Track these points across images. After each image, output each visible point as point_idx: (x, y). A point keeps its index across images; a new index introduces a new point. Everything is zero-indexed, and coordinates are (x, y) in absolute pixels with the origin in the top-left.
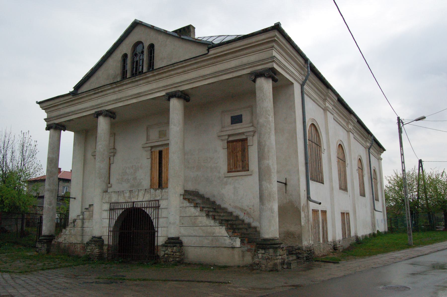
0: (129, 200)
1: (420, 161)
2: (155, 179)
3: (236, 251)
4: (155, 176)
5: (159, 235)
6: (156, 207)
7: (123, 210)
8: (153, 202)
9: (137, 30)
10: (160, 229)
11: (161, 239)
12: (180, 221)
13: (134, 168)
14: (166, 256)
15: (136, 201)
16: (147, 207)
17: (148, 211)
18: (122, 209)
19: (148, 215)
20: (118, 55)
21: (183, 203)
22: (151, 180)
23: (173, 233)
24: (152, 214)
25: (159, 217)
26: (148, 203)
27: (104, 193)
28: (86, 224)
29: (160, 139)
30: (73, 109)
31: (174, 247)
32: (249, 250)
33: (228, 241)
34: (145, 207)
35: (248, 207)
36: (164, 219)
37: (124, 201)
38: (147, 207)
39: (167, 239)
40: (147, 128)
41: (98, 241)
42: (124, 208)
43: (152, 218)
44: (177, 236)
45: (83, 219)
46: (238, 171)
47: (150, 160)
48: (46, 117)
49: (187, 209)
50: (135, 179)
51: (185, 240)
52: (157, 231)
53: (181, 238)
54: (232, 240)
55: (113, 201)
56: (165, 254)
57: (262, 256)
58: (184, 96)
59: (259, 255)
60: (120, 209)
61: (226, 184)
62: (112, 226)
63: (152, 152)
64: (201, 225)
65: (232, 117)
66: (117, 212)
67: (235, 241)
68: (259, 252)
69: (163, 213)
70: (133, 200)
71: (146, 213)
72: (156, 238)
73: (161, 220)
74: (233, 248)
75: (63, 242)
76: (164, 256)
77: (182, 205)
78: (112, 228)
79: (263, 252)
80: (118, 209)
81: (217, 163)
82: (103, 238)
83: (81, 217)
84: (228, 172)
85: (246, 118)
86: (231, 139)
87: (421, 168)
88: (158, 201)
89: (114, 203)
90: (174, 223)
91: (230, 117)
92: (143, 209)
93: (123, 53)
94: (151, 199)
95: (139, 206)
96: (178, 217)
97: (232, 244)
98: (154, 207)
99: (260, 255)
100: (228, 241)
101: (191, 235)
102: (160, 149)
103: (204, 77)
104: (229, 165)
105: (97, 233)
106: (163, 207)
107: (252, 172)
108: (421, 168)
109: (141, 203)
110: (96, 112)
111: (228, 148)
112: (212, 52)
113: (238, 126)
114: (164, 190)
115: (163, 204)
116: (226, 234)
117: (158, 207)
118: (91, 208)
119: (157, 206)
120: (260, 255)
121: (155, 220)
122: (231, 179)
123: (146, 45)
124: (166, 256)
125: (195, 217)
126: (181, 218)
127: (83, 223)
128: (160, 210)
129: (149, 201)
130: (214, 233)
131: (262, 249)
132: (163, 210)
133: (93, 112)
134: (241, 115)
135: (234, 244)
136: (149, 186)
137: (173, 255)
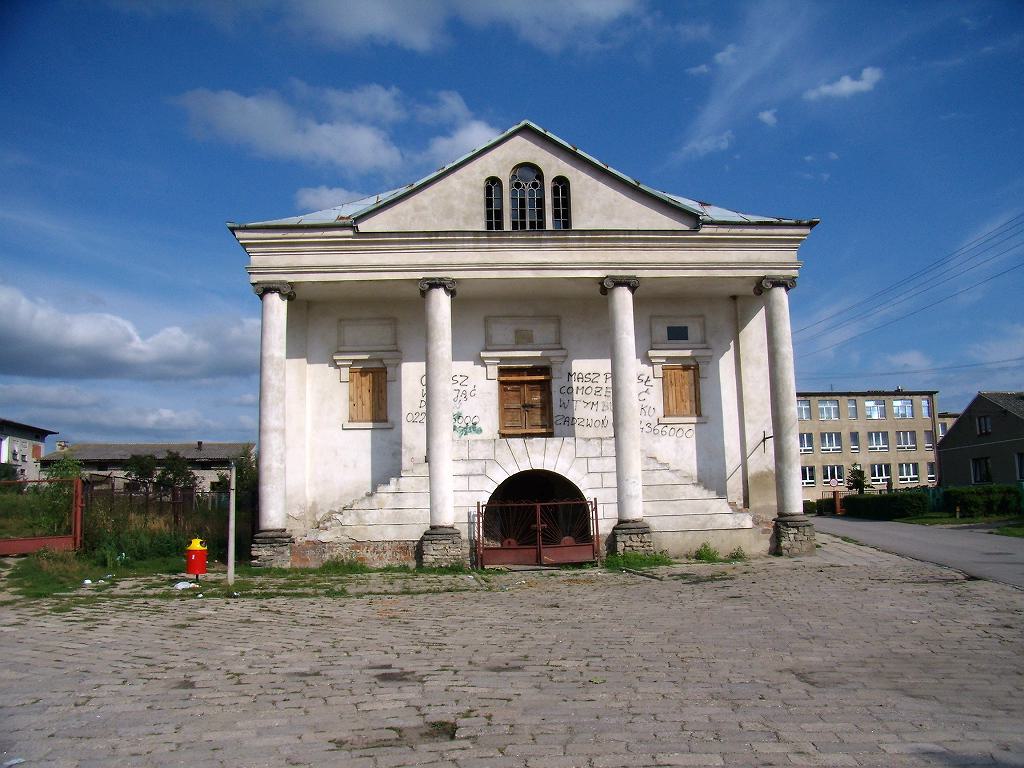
11: (604, 523)
12: (643, 492)
14: (628, 549)
21: (647, 464)
29: (520, 347)
46: (684, 416)
49: (657, 474)
51: (655, 524)
58: (631, 284)
65: (669, 328)
77: (646, 467)
85: (694, 332)
99: (792, 536)
103: (684, 266)
104: (666, 404)
107: (708, 417)
110: (428, 279)
112: (705, 230)
133: (419, 276)
134: (686, 328)
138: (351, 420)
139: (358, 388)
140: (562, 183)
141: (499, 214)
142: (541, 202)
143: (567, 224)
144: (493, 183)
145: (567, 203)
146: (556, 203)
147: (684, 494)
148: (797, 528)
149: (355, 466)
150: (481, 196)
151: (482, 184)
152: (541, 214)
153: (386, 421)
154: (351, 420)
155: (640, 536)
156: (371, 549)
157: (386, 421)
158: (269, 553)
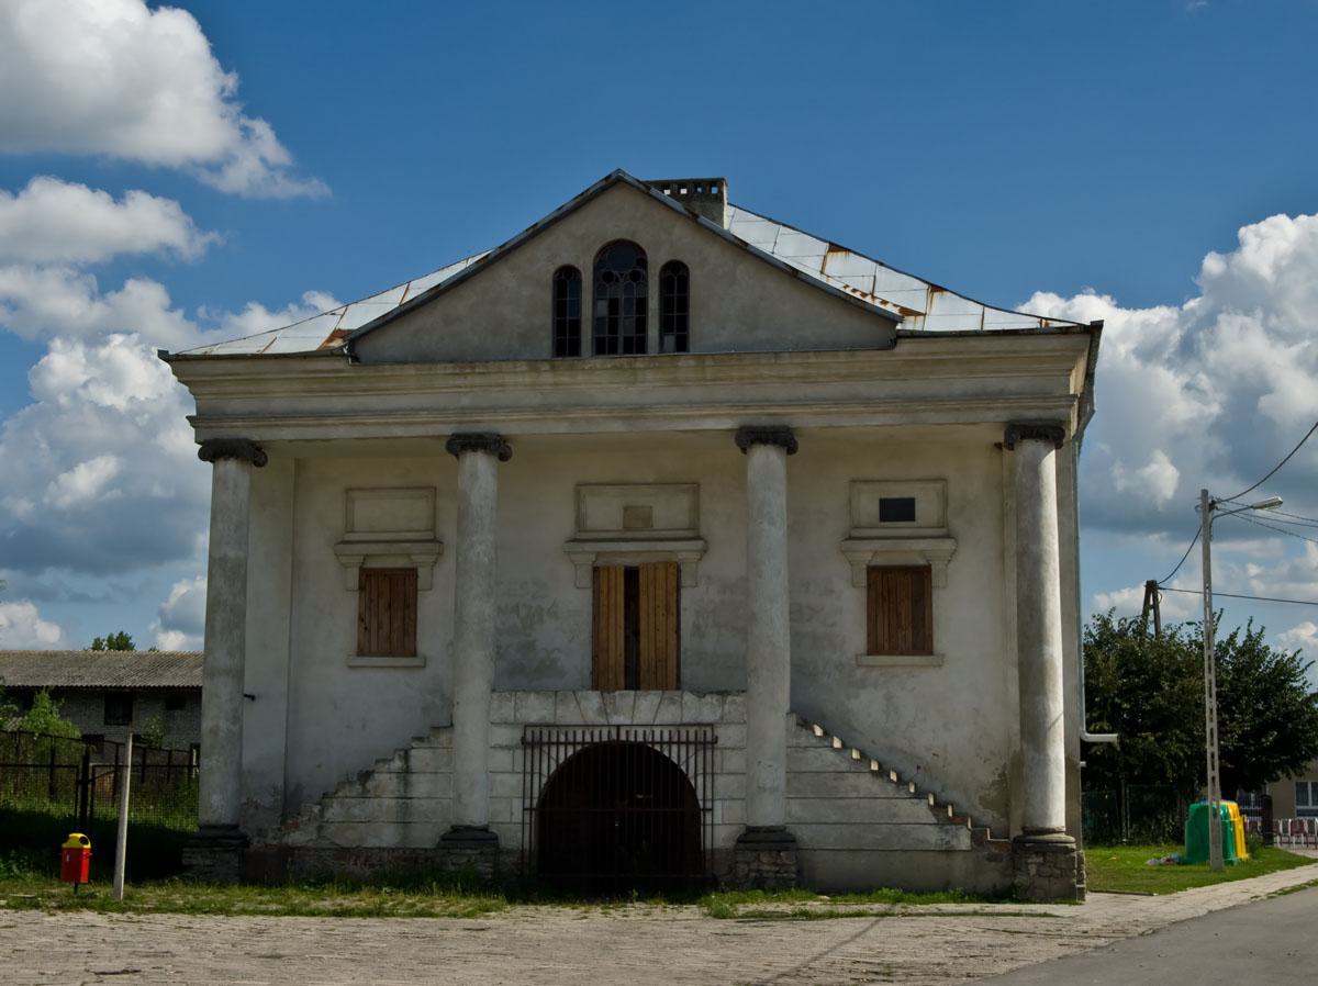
0: (602, 720)
1: (1263, 628)
2: (612, 654)
3: (959, 860)
4: (612, 644)
5: (718, 820)
6: (705, 743)
7: (579, 748)
8: (692, 731)
9: (616, 198)
10: (718, 805)
11: (721, 827)
12: (788, 782)
13: (523, 612)
15: (628, 722)
16: (670, 743)
17: (673, 754)
18: (574, 744)
19: (676, 767)
20: (542, 262)
22: (595, 657)
23: (770, 813)
24: (692, 761)
25: (717, 770)
26: (674, 730)
27: (495, 695)
28: (421, 786)
30: (338, 403)
31: (779, 851)
32: (993, 858)
33: (933, 836)
34: (661, 743)
35: (928, 749)
36: (732, 777)
37: (581, 722)
38: (670, 743)
39: (743, 831)
40: (577, 493)
41: (482, 837)
42: (583, 743)
43: (691, 774)
44: (781, 823)
45: (406, 772)
47: (589, 593)
48: (194, 413)
49: (811, 753)
50: (529, 647)
51: (805, 834)
52: (712, 810)
53: (791, 829)
54: (947, 832)
55: (534, 718)
56: (750, 870)
57: (1038, 870)
59: (1030, 866)
60: (566, 744)
61: (862, 684)
62: (536, 794)
63: (596, 570)
64: (854, 795)
66: (554, 754)
67: (956, 836)
68: (1030, 861)
69: (734, 761)
70: (615, 720)
71: (667, 760)
72: (709, 829)
73: (721, 781)
74: (950, 852)
75: (310, 844)
76: (747, 875)
77: (794, 742)
78: (535, 802)
79: (1041, 860)
80: (558, 744)
81: (832, 625)
82: (493, 829)
83: (397, 764)
84: (870, 653)
86: (880, 561)
87: (1151, 612)
88: (711, 725)
89: (540, 725)
90: (773, 790)
91: (877, 502)
92: (657, 748)
93: (559, 263)
94: (686, 720)
95: (640, 739)
96: (782, 772)
97: (948, 842)
98: (696, 743)
99: (1033, 870)
100: (933, 836)
101: (823, 820)
102: (632, 562)
105: (475, 815)
106: (729, 744)
108: (1151, 612)
109: (648, 730)
111: (869, 585)
112: (904, 347)
113: (902, 528)
114: (730, 698)
115: (727, 735)
116: (934, 820)
117: (706, 743)
118: (443, 737)
119: (709, 738)
120: (1033, 870)
121: (700, 780)
122: (875, 673)
123: (657, 260)
124: (753, 874)
125: (839, 775)
126: (791, 775)
127: (407, 784)
128: (717, 753)
129: (679, 725)
130: (895, 815)
131: (1037, 853)
132: (728, 753)
135: (954, 842)
136: (587, 672)
137: (778, 872)
138: (361, 653)
139: (371, 601)
140: (676, 276)
141: (576, 326)
142: (642, 304)
143: (682, 345)
144: (566, 279)
145: (683, 304)
146: (666, 304)
147: (856, 788)
148: (1044, 854)
149: (364, 727)
150: (547, 298)
151: (548, 277)
152: (641, 325)
153: (414, 654)
154: (361, 653)
155: (774, 854)
156: (362, 859)
157: (414, 654)
158: (208, 862)
